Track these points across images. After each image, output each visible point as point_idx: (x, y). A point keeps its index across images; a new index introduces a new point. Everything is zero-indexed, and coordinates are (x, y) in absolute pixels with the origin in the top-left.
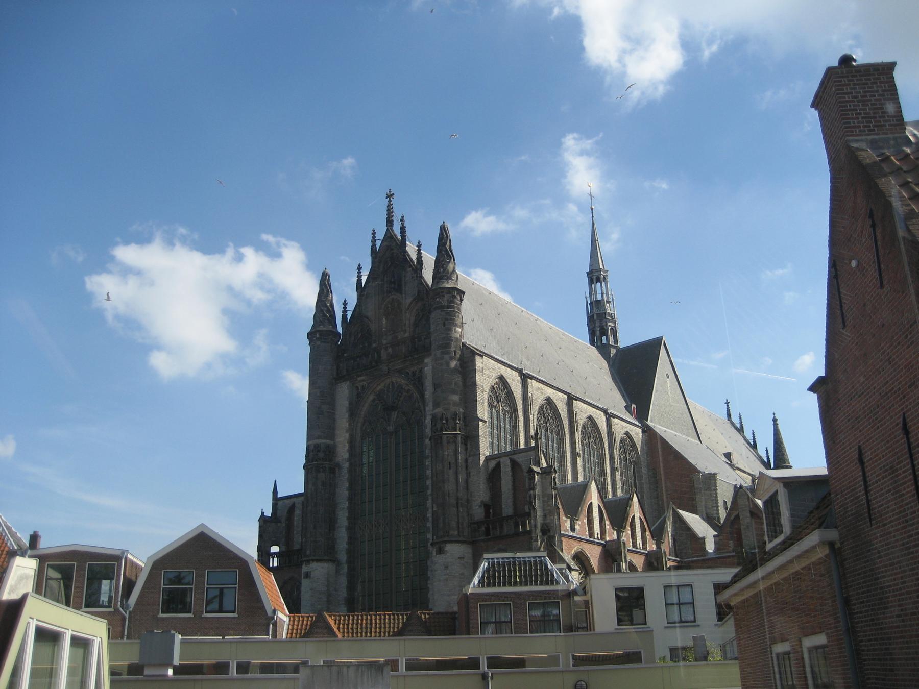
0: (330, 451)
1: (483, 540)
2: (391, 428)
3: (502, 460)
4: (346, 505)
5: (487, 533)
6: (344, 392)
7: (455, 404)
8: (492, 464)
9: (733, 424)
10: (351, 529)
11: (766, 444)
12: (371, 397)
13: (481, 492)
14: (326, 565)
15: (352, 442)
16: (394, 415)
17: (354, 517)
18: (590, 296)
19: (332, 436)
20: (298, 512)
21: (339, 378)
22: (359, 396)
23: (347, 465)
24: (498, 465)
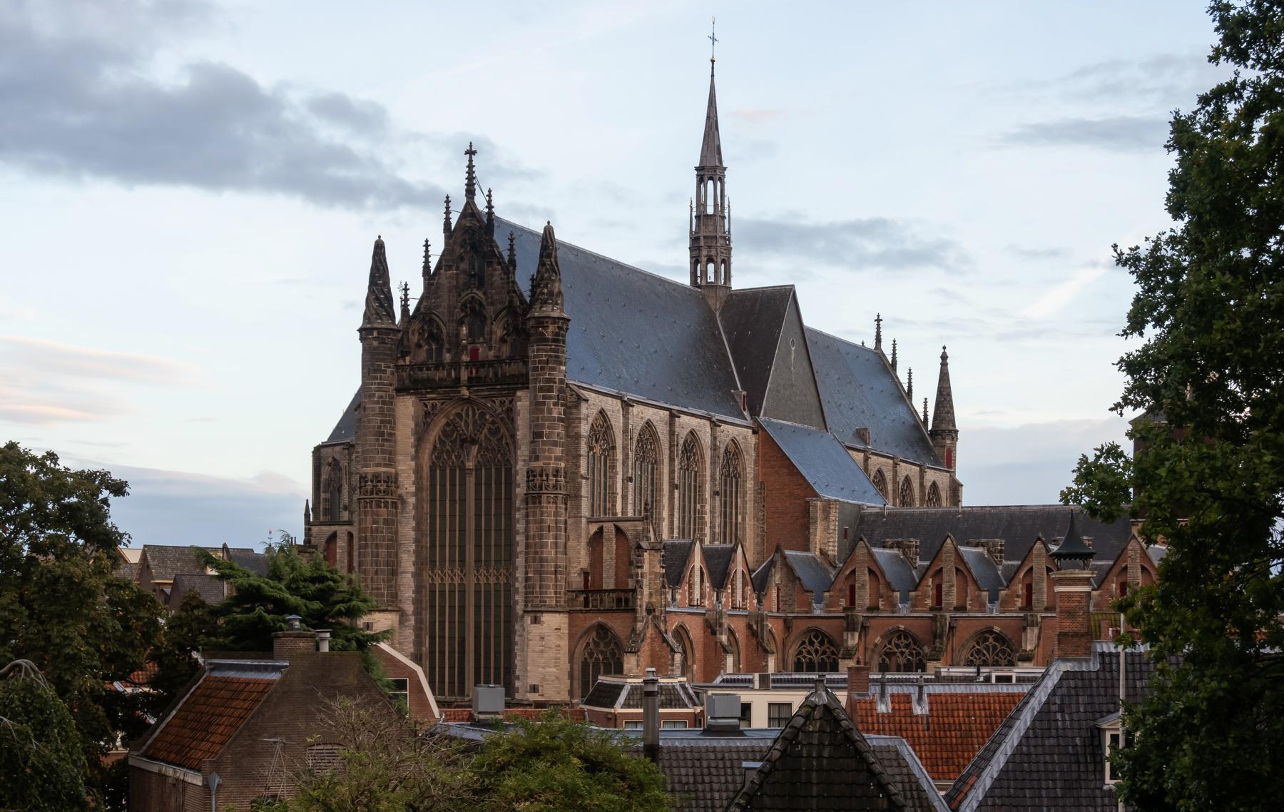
0: (392, 480)
1: (581, 611)
2: (470, 465)
3: (605, 525)
4: (413, 547)
5: (586, 603)
6: (407, 409)
7: (557, 459)
8: (594, 528)
9: (882, 356)
10: (417, 575)
11: (924, 397)
12: (444, 421)
13: (582, 559)
14: (389, 616)
15: (418, 471)
16: (475, 449)
17: (419, 563)
18: (698, 206)
19: (391, 462)
20: (341, 543)
21: (402, 390)
22: (427, 414)
23: (412, 500)
24: (601, 529)
